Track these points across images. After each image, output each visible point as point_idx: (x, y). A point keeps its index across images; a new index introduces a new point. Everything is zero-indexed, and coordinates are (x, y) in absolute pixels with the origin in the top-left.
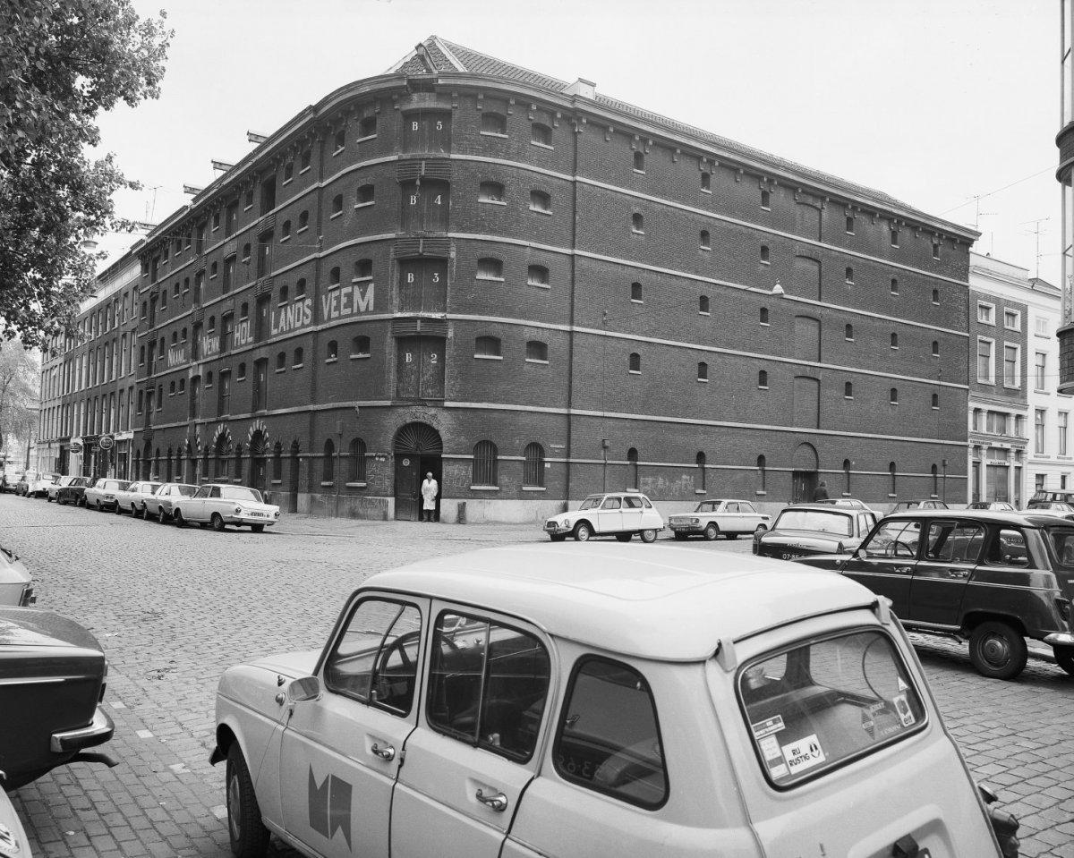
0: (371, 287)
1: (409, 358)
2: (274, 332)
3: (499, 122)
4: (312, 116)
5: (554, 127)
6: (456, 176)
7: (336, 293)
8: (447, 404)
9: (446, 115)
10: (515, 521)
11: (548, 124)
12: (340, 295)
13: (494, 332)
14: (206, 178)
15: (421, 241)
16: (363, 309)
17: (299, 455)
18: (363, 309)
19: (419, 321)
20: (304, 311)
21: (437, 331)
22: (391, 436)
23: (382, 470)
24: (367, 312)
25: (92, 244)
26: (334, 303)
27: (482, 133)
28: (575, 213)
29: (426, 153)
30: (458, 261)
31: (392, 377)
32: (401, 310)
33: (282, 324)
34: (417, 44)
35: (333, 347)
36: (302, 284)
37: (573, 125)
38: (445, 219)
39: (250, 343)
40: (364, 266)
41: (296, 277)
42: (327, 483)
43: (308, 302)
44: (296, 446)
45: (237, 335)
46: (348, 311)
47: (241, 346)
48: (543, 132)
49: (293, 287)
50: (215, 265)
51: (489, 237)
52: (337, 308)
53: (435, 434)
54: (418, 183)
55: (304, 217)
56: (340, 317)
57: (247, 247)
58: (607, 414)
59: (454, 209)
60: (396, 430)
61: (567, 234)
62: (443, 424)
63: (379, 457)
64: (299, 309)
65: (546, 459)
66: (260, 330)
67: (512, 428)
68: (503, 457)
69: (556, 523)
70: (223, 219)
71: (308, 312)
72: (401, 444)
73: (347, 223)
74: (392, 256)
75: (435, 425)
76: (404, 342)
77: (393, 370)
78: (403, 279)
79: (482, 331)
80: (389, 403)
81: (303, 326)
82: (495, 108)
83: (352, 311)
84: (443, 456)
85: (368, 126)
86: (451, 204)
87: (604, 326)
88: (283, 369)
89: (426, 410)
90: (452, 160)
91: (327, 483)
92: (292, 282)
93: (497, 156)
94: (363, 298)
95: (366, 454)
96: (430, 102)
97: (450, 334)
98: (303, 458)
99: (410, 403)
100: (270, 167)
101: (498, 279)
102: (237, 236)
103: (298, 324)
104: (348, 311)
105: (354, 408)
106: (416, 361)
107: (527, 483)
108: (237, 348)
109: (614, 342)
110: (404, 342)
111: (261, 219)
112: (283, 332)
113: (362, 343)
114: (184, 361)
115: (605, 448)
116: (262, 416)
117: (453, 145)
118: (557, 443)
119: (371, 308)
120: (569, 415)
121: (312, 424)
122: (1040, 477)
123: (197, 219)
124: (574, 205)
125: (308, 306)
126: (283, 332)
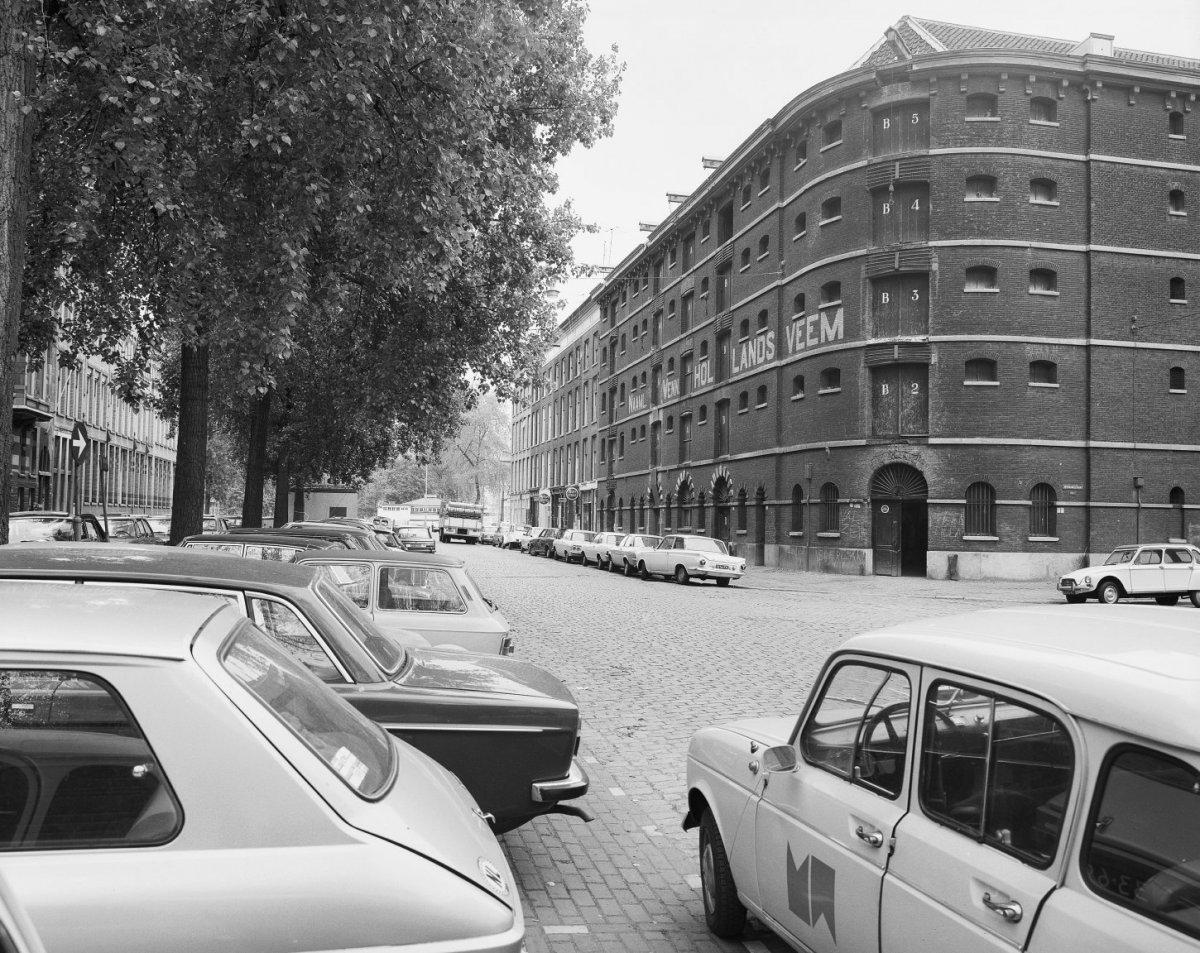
0: (840, 312)
1: (885, 389)
2: (736, 370)
3: (989, 103)
4: (770, 130)
5: (1061, 99)
6: (936, 174)
7: (801, 323)
8: (932, 441)
9: (922, 106)
10: (1020, 578)
12: (805, 325)
13: (989, 353)
14: (661, 212)
15: (897, 255)
17: (765, 503)
19: (896, 347)
21: (918, 357)
22: (866, 479)
23: (857, 518)
24: (836, 340)
25: (555, 293)
26: (799, 334)
28: (1089, 199)
29: (901, 153)
30: (941, 273)
31: (867, 412)
32: (875, 335)
33: (744, 361)
34: (886, 29)
35: (799, 383)
36: (763, 316)
37: (1086, 92)
38: (925, 226)
39: (711, 384)
40: (832, 290)
41: (757, 309)
42: (796, 534)
43: (771, 335)
44: (761, 493)
46: (815, 341)
47: (702, 387)
48: (1046, 107)
49: (754, 320)
50: (672, 303)
51: (978, 242)
52: (803, 339)
53: (918, 475)
54: (891, 188)
55: (764, 242)
56: (806, 349)
57: (705, 282)
58: (1140, 446)
60: (872, 472)
61: (1081, 227)
62: (928, 464)
63: (854, 503)
65: (1058, 503)
66: (721, 369)
68: (1003, 502)
69: (1073, 580)
70: (680, 255)
71: (771, 345)
72: (881, 489)
73: (811, 243)
74: (863, 275)
75: (918, 465)
76: (879, 372)
77: (868, 404)
78: (877, 299)
79: (973, 354)
80: (863, 442)
81: (766, 361)
82: (982, 88)
84: (928, 501)
85: (833, 131)
87: (1133, 335)
88: (746, 410)
89: (907, 448)
90: (931, 156)
91: (796, 534)
92: (753, 314)
93: (987, 144)
94: (831, 325)
95: (839, 501)
96: (903, 93)
97: (934, 359)
98: (769, 505)
99: (888, 442)
100: (728, 192)
101: (991, 290)
102: (694, 271)
103: (760, 360)
104: (815, 341)
105: (824, 449)
106: (894, 393)
107: (1035, 532)
108: (697, 389)
109: (1147, 356)
110: (879, 372)
111: (718, 249)
112: (744, 370)
113: (832, 376)
115: (1138, 487)
116: (725, 462)
117: (932, 138)
118: (1072, 484)
119: (841, 336)
120: (1087, 449)
121: (778, 469)
123: (653, 256)
124: (1088, 188)
126: (744, 370)
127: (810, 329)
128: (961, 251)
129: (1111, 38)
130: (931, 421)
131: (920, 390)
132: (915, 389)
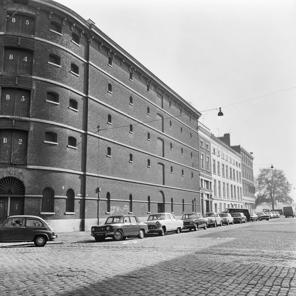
5: (81, 37)
9: (32, 18)
21: (23, 127)
27: (51, 30)
53: (20, 184)
58: (100, 175)
59: (35, 64)
67: (61, 181)
75: (21, 178)
82: (57, 21)
86: (34, 61)
89: (16, 169)
93: (57, 43)
97: (32, 129)
117: (36, 33)
122: (216, 204)
128: (45, 83)
129: (95, 23)
130: (28, 158)
131: (22, 142)
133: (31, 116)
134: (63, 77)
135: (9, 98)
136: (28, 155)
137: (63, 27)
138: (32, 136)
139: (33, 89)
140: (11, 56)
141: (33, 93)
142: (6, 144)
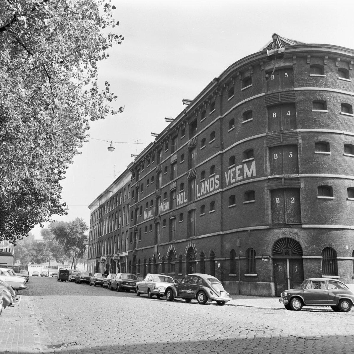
0: (254, 163)
1: (278, 201)
2: (198, 195)
4: (216, 83)
5: (351, 70)
7: (234, 169)
9: (290, 69)
11: (347, 68)
12: (236, 170)
14: (161, 126)
16: (249, 176)
17: (215, 259)
18: (249, 176)
20: (214, 181)
21: (294, 185)
22: (271, 246)
24: (252, 177)
25: (112, 149)
26: (232, 175)
27: (311, 75)
29: (281, 90)
30: (303, 144)
31: (270, 212)
33: (203, 190)
34: (272, 34)
35: (233, 199)
36: (213, 168)
39: (186, 203)
40: (249, 153)
41: (210, 165)
42: (233, 275)
43: (217, 176)
44: (213, 255)
45: (178, 200)
46: (241, 178)
47: (181, 205)
49: (208, 171)
50: (166, 168)
52: (234, 177)
53: (297, 244)
55: (213, 135)
56: (236, 182)
57: (183, 156)
59: (299, 116)
60: (273, 242)
63: (264, 258)
64: (212, 181)
66: (190, 196)
67: (343, 239)
70: (170, 146)
71: (217, 182)
73: (237, 132)
74: (265, 145)
75: (297, 239)
76: (274, 192)
77: (270, 208)
78: (271, 157)
81: (215, 190)
82: (318, 62)
83: (243, 178)
85: (247, 81)
86: (297, 113)
88: (204, 214)
89: (291, 230)
91: (233, 275)
92: (207, 169)
93: (321, 86)
94: (249, 170)
95: (256, 257)
96: (281, 64)
97: (302, 185)
98: (217, 260)
100: (194, 114)
102: (177, 152)
103: (212, 189)
104: (241, 178)
105: (247, 231)
106: (283, 202)
108: (179, 206)
110: (274, 192)
111: (189, 141)
112: (203, 195)
113: (250, 194)
114: (152, 216)
116: (192, 240)
117: (295, 83)
119: (254, 175)
121: (222, 243)
123: (157, 148)
125: (217, 179)
127: (238, 172)
128: (312, 134)
131: (295, 201)
132: (293, 200)
133: (300, 172)
134: (331, 122)
135: (277, 157)
136: (302, 213)
137: (325, 66)
138: (304, 193)
139: (299, 143)
140: (274, 114)
141: (300, 147)
142: (279, 204)
